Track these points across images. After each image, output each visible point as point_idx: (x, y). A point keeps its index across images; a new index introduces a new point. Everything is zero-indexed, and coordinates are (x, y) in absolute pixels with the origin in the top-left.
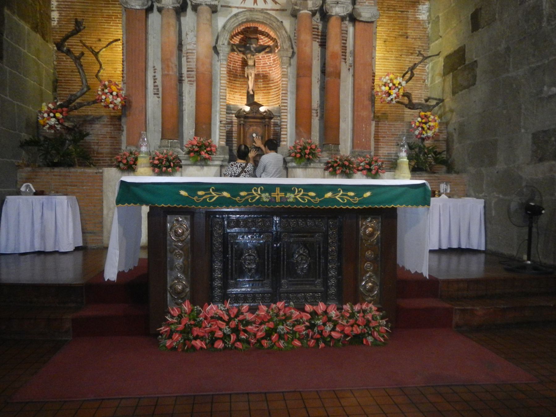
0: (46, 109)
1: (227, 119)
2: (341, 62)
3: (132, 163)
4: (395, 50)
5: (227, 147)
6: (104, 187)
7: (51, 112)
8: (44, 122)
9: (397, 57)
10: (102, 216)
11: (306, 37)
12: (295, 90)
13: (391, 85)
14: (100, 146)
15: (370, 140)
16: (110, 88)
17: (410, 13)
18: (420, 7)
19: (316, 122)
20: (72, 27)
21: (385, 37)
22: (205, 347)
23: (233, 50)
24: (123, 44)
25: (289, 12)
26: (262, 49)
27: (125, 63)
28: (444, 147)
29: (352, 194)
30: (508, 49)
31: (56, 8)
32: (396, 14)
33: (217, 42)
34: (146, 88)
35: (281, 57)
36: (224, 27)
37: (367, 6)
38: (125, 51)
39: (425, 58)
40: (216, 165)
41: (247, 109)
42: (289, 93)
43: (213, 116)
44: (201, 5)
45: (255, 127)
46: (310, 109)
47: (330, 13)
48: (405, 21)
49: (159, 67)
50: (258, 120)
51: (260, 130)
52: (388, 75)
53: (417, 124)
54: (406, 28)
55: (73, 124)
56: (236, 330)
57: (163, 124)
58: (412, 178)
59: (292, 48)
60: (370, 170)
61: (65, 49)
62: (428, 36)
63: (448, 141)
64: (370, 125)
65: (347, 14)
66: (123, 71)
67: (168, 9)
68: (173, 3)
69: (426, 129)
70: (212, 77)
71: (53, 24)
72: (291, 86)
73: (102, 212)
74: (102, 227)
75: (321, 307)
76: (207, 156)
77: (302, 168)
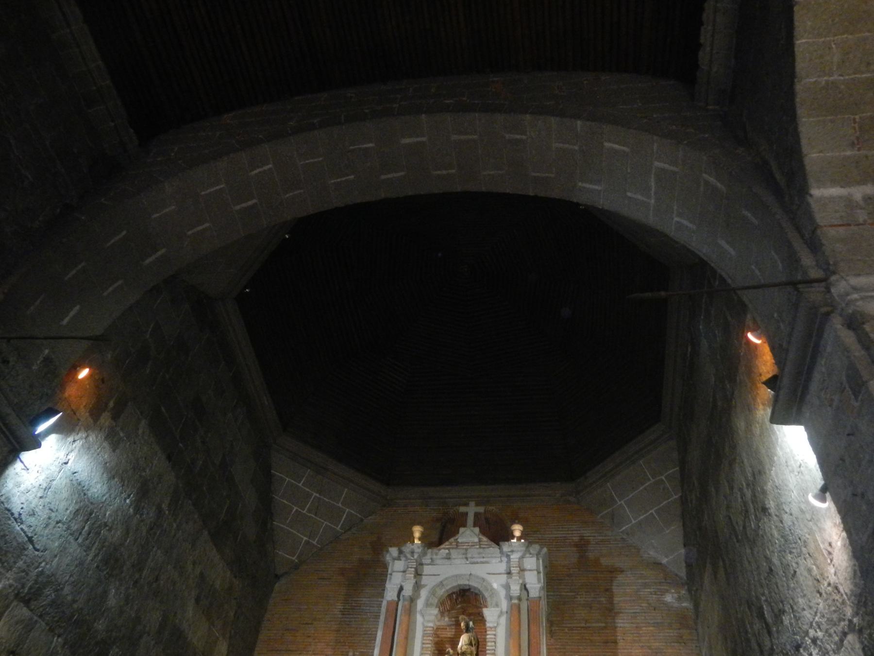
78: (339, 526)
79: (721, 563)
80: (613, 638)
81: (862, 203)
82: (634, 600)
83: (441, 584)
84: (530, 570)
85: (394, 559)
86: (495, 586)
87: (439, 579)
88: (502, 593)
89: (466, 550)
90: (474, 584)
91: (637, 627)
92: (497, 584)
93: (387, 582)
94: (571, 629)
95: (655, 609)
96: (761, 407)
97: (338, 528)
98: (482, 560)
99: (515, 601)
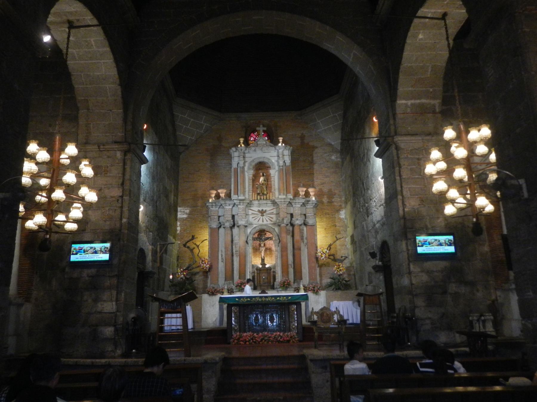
2: (300, 244)
7: (182, 272)
10: (201, 315)
11: (284, 235)
12: (281, 257)
13: (322, 253)
18: (341, 212)
19: (291, 270)
20: (191, 238)
22: (243, 343)
25: (277, 224)
26: (268, 239)
28: (353, 277)
29: (285, 298)
30: (361, 239)
31: (180, 225)
33: (247, 239)
34: (218, 259)
35: (275, 243)
36: (250, 233)
37: (311, 219)
39: (337, 240)
41: (261, 266)
43: (246, 270)
45: (264, 274)
46: (288, 265)
47: (294, 224)
49: (224, 250)
50: (265, 271)
51: (266, 275)
52: (320, 248)
53: (335, 269)
54: (335, 222)
56: (252, 339)
57: (225, 274)
58: (305, 292)
59: (279, 239)
60: (314, 290)
62: (346, 225)
63: (354, 275)
64: (316, 270)
67: (227, 227)
72: (279, 255)
73: (201, 313)
74: (201, 319)
75: (278, 333)
78: (202, 131)
79: (353, 160)
83: (253, 161)
84: (286, 155)
85: (234, 152)
86: (273, 161)
87: (252, 159)
88: (276, 163)
89: (262, 148)
90: (266, 161)
92: (274, 160)
94: (298, 170)
99: (282, 168)
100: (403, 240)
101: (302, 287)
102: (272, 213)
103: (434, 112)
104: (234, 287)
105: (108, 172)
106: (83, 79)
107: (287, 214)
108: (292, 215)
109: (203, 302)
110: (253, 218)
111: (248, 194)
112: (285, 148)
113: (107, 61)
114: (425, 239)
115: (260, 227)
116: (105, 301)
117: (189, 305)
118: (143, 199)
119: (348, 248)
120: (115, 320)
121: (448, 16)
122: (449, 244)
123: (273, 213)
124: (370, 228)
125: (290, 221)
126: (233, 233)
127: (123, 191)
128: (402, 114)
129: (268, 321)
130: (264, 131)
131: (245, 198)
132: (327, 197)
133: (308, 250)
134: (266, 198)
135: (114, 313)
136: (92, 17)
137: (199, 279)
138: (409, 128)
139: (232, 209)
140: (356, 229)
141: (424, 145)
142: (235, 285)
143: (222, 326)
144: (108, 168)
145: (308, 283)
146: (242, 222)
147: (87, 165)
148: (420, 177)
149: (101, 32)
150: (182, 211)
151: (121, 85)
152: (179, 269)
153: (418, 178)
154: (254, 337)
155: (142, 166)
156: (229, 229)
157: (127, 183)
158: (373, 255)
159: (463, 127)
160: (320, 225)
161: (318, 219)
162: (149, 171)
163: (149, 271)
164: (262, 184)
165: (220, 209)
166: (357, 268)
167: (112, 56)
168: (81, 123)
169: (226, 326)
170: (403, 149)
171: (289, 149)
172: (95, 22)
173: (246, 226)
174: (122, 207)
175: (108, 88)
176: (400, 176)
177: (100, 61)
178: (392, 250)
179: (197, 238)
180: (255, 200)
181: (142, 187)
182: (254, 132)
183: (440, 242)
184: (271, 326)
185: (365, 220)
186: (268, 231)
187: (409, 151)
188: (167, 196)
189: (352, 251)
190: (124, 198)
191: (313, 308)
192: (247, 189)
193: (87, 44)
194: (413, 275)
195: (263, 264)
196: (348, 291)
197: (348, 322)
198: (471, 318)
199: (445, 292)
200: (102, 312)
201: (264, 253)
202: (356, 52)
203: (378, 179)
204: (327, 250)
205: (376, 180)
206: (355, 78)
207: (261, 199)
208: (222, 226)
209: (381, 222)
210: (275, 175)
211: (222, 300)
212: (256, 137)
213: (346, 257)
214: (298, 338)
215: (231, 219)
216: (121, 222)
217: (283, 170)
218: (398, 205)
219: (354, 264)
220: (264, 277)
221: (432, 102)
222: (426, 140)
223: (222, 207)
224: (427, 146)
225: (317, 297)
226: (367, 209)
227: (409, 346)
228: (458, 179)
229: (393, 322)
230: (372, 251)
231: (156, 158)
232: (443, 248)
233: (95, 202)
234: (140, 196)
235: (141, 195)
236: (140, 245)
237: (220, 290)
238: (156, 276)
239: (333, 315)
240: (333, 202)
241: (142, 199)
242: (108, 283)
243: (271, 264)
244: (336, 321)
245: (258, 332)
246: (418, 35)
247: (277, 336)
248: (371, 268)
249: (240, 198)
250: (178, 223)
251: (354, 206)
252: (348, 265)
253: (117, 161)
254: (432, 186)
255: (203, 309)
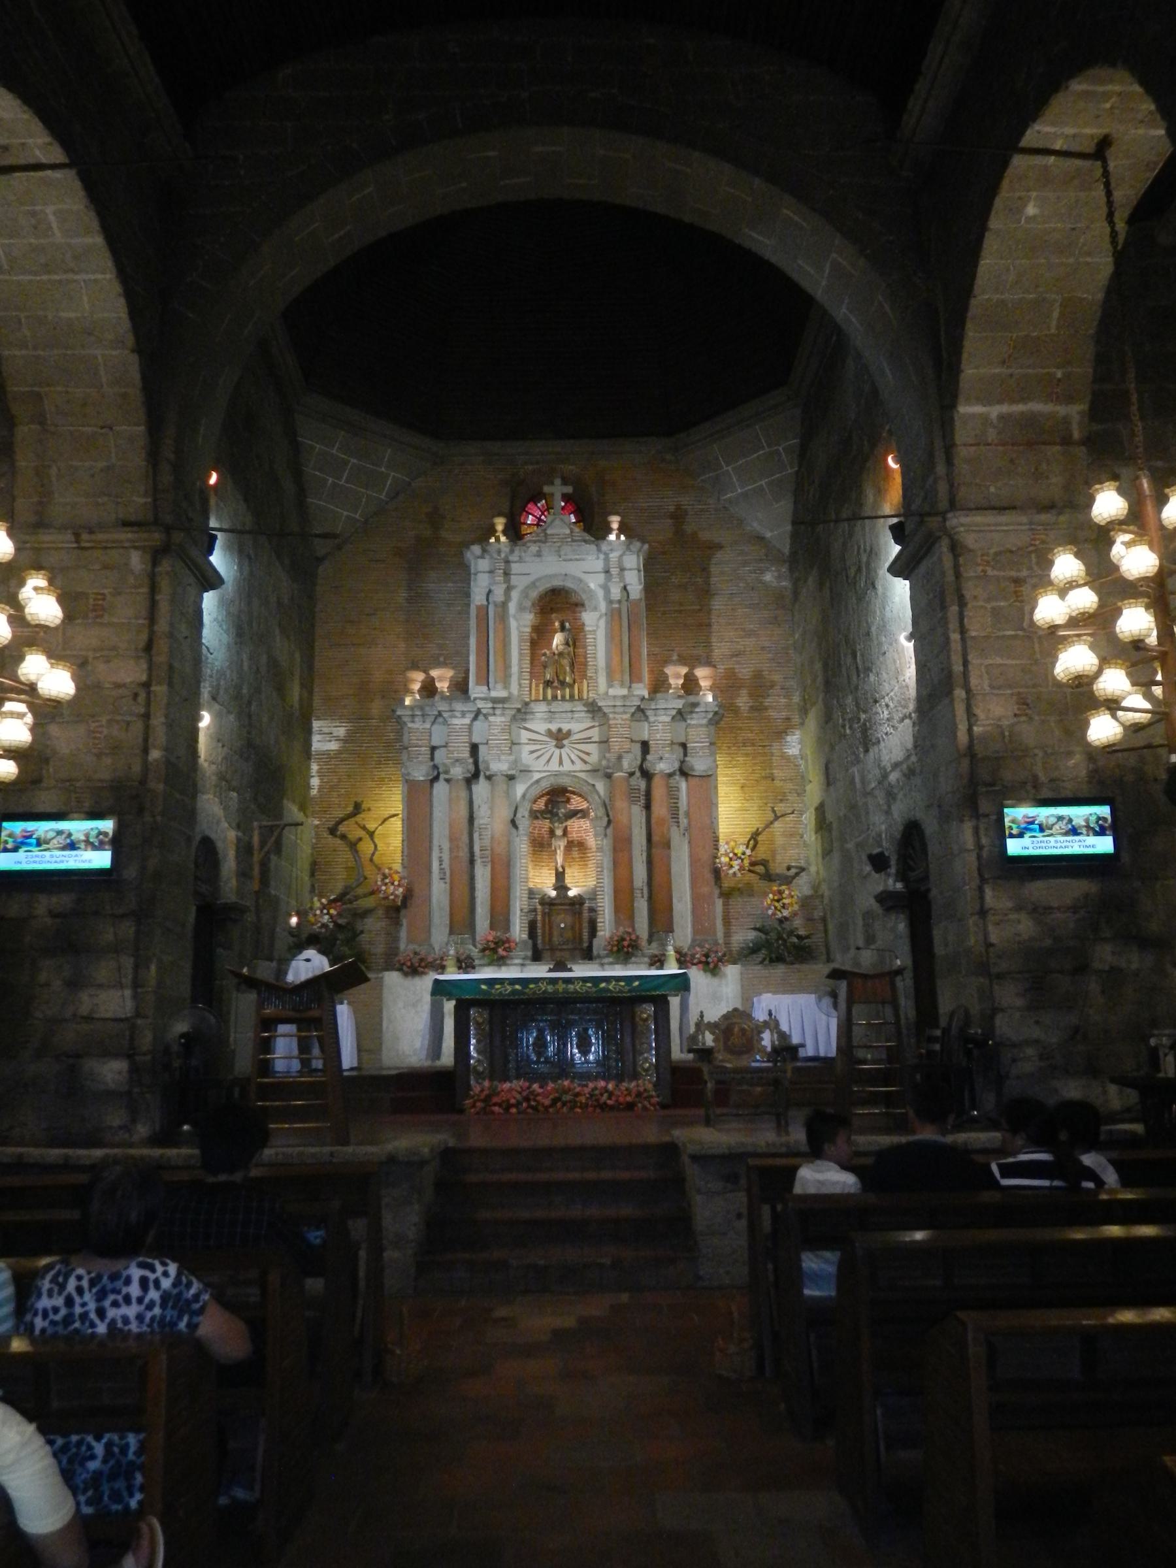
0: (317, 904)
1: (529, 905)
2: (669, 830)
3: (417, 964)
4: (757, 797)
5: (530, 942)
6: (385, 995)
7: (324, 908)
8: (316, 920)
9: (761, 807)
10: (381, 1031)
13: (731, 855)
14: (373, 944)
15: (715, 924)
16: (392, 877)
17: (775, 747)
18: (789, 738)
19: (642, 907)
20: (350, 809)
21: (743, 781)
22: (501, 1111)
23: (537, 818)
24: (403, 820)
26: (574, 814)
27: (405, 843)
28: (821, 927)
29: (623, 984)
30: (845, 816)
31: (318, 772)
32: (755, 750)
34: (430, 872)
35: (594, 827)
36: (524, 796)
37: (701, 757)
38: (405, 829)
39: (777, 818)
40: (515, 965)
41: (553, 893)
42: (605, 871)
43: (511, 903)
44: (496, 775)
46: (632, 890)
47: (652, 771)
48: (769, 758)
49: (446, 846)
51: (569, 919)
52: (727, 843)
53: (769, 902)
54: (771, 767)
55: (345, 920)
56: (527, 1099)
57: (451, 915)
58: (680, 969)
59: (608, 816)
60: (707, 963)
61: (339, 833)
62: (803, 777)
63: (824, 920)
64: (714, 902)
65: (675, 771)
66: (402, 852)
67: (458, 780)
68: (463, 773)
69: (779, 908)
70: (509, 856)
71: (312, 794)
72: (607, 862)
74: (381, 1044)
75: (602, 1084)
76: (504, 953)
77: (621, 964)
78: (384, 494)
79: (828, 584)
80: (707, 621)
81: (995, 421)
82: (732, 580)
83: (533, 584)
84: (630, 569)
85: (478, 558)
86: (592, 586)
88: (600, 594)
90: (569, 584)
91: (732, 609)
92: (594, 583)
93: (472, 583)
94: (664, 613)
95: (753, 589)
96: (888, 504)
97: (383, 497)
98: (577, 557)
99: (616, 606)
100: (966, 818)
101: (671, 952)
102: (587, 741)
103: (1066, 441)
104: (475, 952)
105: (104, 609)
106: (28, 333)
107: (632, 741)
108: (645, 746)
109: (386, 993)
110: (532, 752)
111: (516, 683)
112: (628, 548)
113: (100, 276)
114: (1031, 815)
115: (552, 780)
116: (100, 986)
117: (346, 1002)
118: (209, 692)
119: (808, 842)
120: (132, 1039)
121: (1113, 149)
122: (1097, 829)
123: (590, 738)
124: (873, 785)
125: (639, 762)
126: (474, 797)
127: (150, 669)
128: (971, 445)
129: (572, 1048)
130: (565, 497)
131: (510, 693)
132: (751, 695)
133: (690, 852)
134: (572, 696)
135: (127, 1019)
136: (48, 139)
137: (373, 926)
138: (992, 489)
139: (470, 726)
140: (832, 788)
141: (1034, 539)
142: (480, 946)
143: (438, 1063)
144: (104, 599)
145: (689, 941)
146: (499, 766)
147: (42, 589)
148: (1020, 633)
149: (77, 184)
150: (326, 730)
151: (139, 350)
152: (316, 899)
153: (1015, 637)
154: (532, 1093)
155: (206, 595)
156: (463, 784)
157: (162, 645)
158: (879, 862)
159: (1149, 487)
160: (727, 775)
161: (721, 760)
162: (229, 613)
163: (229, 901)
164: (561, 654)
165: (435, 727)
166: (831, 900)
167: (110, 264)
168: (21, 463)
169: (453, 1063)
170: (970, 551)
171: (640, 551)
172: (57, 154)
173: (511, 778)
174: (147, 716)
175: (100, 359)
176: (963, 631)
177: (76, 277)
178: (933, 848)
179: (369, 809)
180: (536, 700)
181: (207, 658)
182: (535, 499)
183: (1073, 823)
184: (582, 1063)
185: (858, 761)
186: (573, 793)
187: (989, 559)
188: (281, 689)
189: (820, 851)
190: (153, 688)
191: (702, 1012)
192: (515, 669)
193: (33, 221)
194: (993, 918)
195: (561, 887)
196: (805, 967)
197: (802, 1053)
198: (1153, 1042)
199: (1082, 969)
200: (93, 1018)
201: (565, 854)
202: (840, 260)
203: (896, 641)
204: (747, 847)
205: (891, 644)
206: (834, 338)
207: (555, 698)
208: (442, 777)
209: (905, 766)
210: (597, 626)
211: (440, 989)
212: (543, 514)
213: (802, 869)
214: (658, 1096)
215: (466, 754)
216: (147, 759)
217: (620, 618)
218: (954, 716)
219: (824, 889)
220: (562, 925)
221: (1061, 410)
222: (1040, 525)
223: (440, 720)
224: (1043, 542)
225: (715, 981)
226: (865, 730)
227: (974, 1120)
228: (1131, 639)
229: (930, 1053)
230: (876, 851)
231: (246, 573)
232: (1080, 841)
233: (68, 698)
234: (202, 684)
235: (205, 680)
236: (204, 826)
237: (436, 960)
238: (250, 918)
239: (760, 1032)
240: (766, 709)
241: (205, 692)
242: (108, 935)
243: (585, 889)
244: (769, 1049)
245: (542, 1079)
246: (1026, 206)
247: (597, 1092)
248: (872, 901)
249: (494, 694)
250: (314, 767)
251: (827, 718)
252: (807, 891)
253: (131, 580)
254: (1055, 659)
255: (385, 1013)
